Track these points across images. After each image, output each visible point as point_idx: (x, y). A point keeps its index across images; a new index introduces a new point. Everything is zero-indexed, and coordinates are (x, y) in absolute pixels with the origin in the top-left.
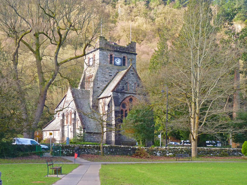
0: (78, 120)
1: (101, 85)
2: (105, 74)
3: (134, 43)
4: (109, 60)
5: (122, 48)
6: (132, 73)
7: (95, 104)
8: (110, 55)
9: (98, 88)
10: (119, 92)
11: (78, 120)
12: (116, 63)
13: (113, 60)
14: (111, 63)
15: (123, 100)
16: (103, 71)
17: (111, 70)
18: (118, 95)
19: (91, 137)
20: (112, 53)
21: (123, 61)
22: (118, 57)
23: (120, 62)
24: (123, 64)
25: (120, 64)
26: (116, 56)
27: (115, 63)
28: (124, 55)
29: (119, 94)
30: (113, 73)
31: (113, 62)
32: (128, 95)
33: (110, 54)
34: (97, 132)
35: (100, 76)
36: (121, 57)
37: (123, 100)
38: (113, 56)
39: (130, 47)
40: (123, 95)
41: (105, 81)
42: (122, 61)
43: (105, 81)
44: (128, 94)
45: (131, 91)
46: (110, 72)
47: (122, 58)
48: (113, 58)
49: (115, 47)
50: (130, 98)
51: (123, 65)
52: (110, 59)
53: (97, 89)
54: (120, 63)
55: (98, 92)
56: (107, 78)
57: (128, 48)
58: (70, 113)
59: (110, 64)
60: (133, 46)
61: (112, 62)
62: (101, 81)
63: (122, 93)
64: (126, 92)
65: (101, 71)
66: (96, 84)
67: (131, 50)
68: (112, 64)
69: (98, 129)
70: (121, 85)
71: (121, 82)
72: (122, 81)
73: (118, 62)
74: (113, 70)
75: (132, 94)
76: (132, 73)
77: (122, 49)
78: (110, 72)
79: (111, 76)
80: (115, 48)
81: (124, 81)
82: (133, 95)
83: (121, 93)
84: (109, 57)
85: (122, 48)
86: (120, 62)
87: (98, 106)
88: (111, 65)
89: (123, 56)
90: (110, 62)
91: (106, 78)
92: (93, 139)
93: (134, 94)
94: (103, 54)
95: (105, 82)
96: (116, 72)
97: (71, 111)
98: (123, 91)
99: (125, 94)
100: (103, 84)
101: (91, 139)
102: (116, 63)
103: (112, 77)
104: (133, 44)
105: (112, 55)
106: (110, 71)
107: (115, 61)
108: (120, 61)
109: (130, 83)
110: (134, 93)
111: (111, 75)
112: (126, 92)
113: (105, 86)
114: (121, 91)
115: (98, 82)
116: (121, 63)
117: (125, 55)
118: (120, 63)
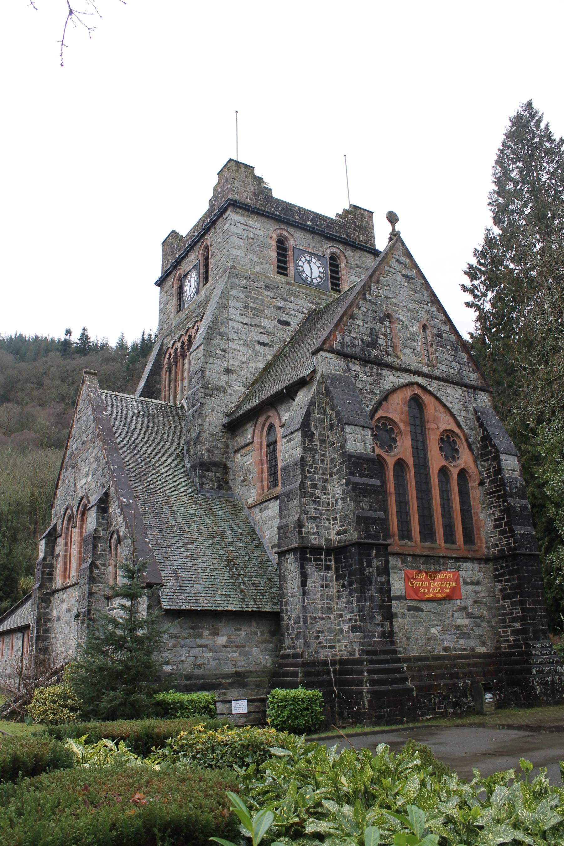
0: (119, 541)
1: (244, 359)
2: (258, 313)
3: (366, 213)
4: (274, 255)
5: (322, 222)
6: (403, 275)
7: (213, 453)
8: (275, 236)
9: (228, 371)
10: (356, 358)
11: (119, 541)
12: (304, 275)
13: (290, 258)
14: (282, 269)
15: (378, 406)
16: (247, 297)
17: (284, 299)
18: (349, 369)
19: (199, 641)
20: (285, 233)
21: (331, 270)
22: (310, 251)
23: (320, 272)
24: (332, 283)
25: (319, 280)
26: (301, 247)
27: (299, 273)
28: (335, 250)
29: (356, 367)
30: (292, 312)
31: (291, 266)
32: (401, 381)
33: (278, 232)
34: (238, 609)
35: (235, 318)
36: (320, 254)
37: (378, 406)
38: (291, 243)
39: (354, 223)
40: (375, 377)
41: (261, 344)
42: (325, 269)
43: (261, 344)
44: (399, 374)
45: (409, 359)
46: (280, 305)
47: (328, 256)
48: (290, 253)
49: (297, 212)
50: (409, 393)
51: (332, 289)
52: (278, 254)
53: (224, 378)
54: (319, 277)
55: (229, 391)
56: (269, 330)
57: (346, 224)
58: (79, 516)
59: (279, 273)
60: (362, 221)
61: (286, 269)
62: (240, 339)
63: (371, 362)
64: (390, 360)
65: (242, 295)
66: (218, 352)
67: (358, 237)
68: (286, 275)
69: (242, 591)
70: (360, 322)
71: (359, 309)
72: (364, 306)
73: (313, 270)
74: (293, 299)
75: (417, 373)
76: (404, 272)
77: (322, 225)
78: (279, 308)
79: (287, 324)
80: (297, 217)
81: (374, 304)
82: (420, 380)
83: (365, 361)
84: (274, 243)
85: (324, 220)
86: (320, 272)
87: (229, 464)
88: (282, 278)
89: (328, 252)
90: (279, 267)
91: (262, 331)
92: (209, 655)
93: (424, 375)
94: (246, 227)
95: (258, 348)
96: (306, 311)
97: (85, 500)
98: (374, 352)
99: (385, 372)
100: (249, 359)
101: (200, 661)
102: (304, 275)
103: (290, 328)
104: (362, 215)
105: (286, 239)
106: (280, 303)
107: (301, 263)
108: (321, 269)
109: (403, 318)
110: (425, 369)
111: (284, 318)
112: (389, 362)
113: (262, 366)
114: (363, 350)
115: (230, 344)
116: (322, 275)
117: (338, 249)
118: (319, 277)
